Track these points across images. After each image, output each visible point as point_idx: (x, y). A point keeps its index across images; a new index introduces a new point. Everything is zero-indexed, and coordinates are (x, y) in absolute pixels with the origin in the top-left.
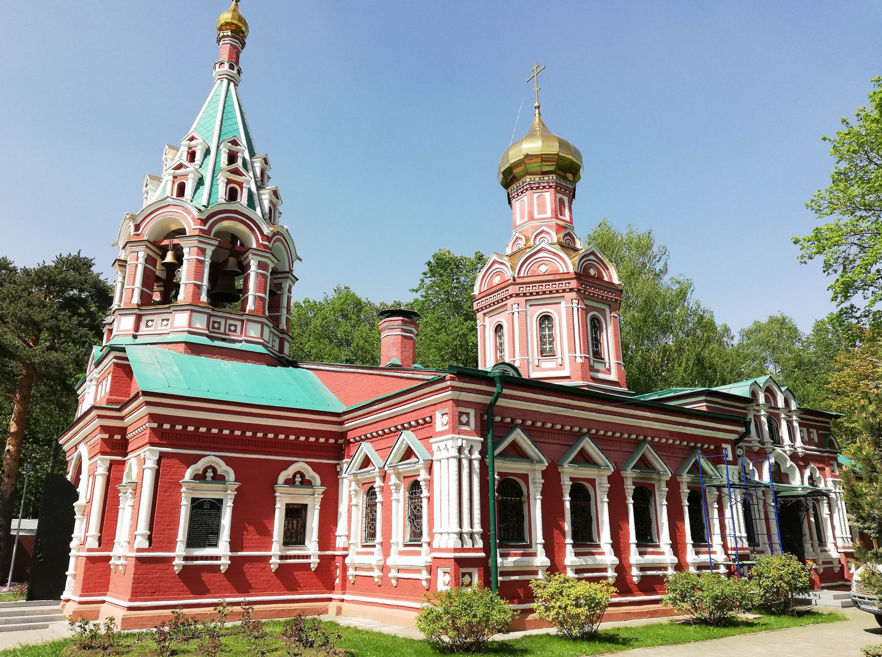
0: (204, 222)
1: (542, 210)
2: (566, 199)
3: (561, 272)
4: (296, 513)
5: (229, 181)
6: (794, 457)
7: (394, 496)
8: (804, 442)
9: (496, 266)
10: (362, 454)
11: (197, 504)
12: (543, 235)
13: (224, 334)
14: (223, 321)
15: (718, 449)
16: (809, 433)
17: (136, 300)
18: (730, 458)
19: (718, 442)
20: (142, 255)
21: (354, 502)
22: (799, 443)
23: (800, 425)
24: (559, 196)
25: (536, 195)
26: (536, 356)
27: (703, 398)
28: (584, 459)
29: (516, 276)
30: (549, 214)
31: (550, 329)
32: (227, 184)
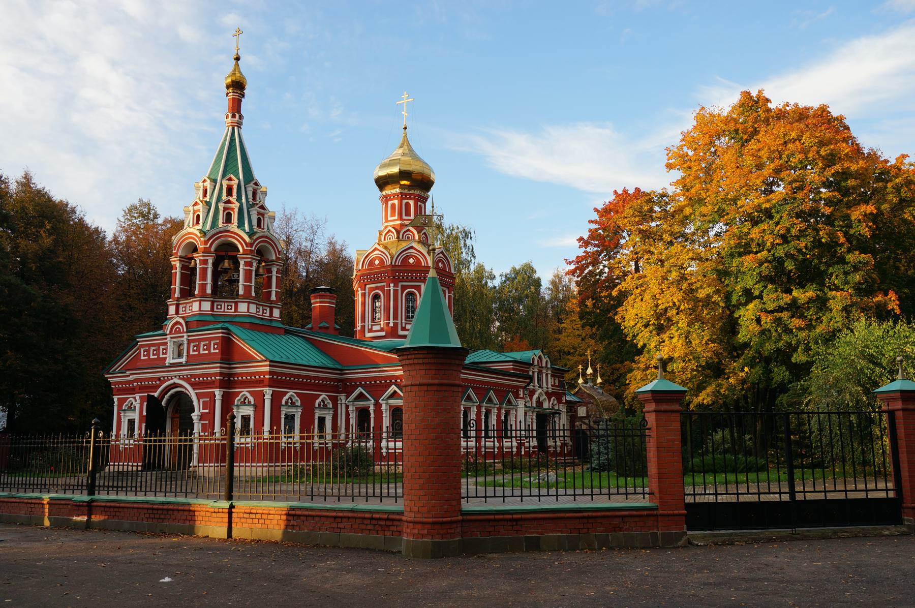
0: (251, 245)
1: (408, 214)
2: (423, 205)
3: (423, 265)
4: (322, 420)
5: (259, 214)
6: (547, 393)
7: (384, 415)
8: (552, 385)
9: (377, 252)
10: (358, 393)
11: (287, 417)
12: (408, 233)
13: (262, 315)
14: (261, 308)
15: (518, 391)
16: (554, 380)
17: (209, 291)
18: (521, 396)
19: (518, 388)
20: (210, 261)
21: (351, 416)
22: (550, 386)
23: (552, 376)
24: (419, 203)
25: (404, 201)
26: (403, 321)
27: (511, 364)
28: (469, 399)
29: (393, 264)
30: (412, 217)
31: (413, 302)
32: (258, 215)
